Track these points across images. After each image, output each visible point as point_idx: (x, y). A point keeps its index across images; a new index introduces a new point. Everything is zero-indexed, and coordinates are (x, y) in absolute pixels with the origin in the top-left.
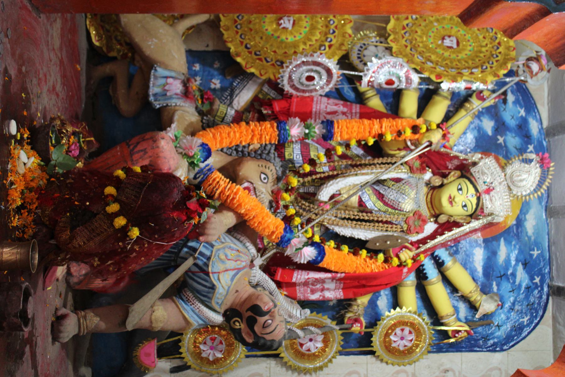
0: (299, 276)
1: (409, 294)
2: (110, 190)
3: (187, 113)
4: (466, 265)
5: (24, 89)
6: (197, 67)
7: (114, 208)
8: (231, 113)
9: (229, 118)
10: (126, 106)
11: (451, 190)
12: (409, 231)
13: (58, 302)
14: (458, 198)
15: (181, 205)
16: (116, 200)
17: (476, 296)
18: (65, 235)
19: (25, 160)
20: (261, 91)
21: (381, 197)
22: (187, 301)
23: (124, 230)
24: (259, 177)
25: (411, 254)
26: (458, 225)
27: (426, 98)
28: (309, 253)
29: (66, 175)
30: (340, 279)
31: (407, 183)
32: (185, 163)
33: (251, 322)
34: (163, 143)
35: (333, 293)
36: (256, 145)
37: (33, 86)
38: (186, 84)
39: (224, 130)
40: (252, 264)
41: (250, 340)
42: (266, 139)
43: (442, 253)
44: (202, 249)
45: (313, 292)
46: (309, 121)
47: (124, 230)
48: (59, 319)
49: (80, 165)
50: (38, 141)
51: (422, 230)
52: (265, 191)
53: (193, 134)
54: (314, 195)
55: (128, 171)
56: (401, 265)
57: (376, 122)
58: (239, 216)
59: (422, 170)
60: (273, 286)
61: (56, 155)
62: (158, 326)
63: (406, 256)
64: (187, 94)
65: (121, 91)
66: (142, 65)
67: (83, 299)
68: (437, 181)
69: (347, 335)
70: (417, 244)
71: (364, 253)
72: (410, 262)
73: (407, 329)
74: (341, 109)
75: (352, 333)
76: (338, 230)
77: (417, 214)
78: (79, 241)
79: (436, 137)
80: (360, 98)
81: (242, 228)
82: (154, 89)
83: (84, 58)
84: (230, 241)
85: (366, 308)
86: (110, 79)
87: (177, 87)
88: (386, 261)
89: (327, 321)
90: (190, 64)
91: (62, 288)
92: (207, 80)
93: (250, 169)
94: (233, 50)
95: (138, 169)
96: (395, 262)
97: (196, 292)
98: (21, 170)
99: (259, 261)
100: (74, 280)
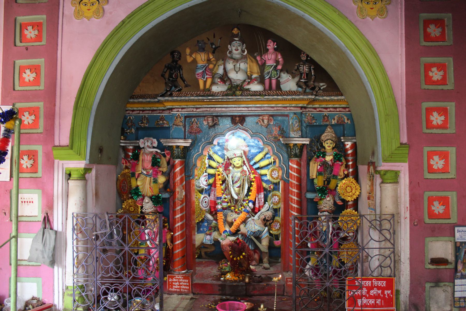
0: (257, 206)
1: (263, 172)
2: (235, 259)
3: (215, 234)
4: (256, 155)
5: (214, 276)
6: (201, 229)
7: (238, 258)
8: (214, 222)
9: (216, 222)
10: (213, 249)
11: (235, 164)
12: (246, 175)
13: (261, 268)
14: (237, 162)
15: (238, 244)
16: (237, 258)
17: (264, 153)
18: (244, 268)
19: (229, 276)
20: (208, 212)
21: (236, 182)
22: (262, 237)
23: (243, 256)
24: (232, 216)
25: (252, 175)
26: (244, 161)
27: (210, 167)
28: (251, 205)
29: (232, 268)
30: (258, 194)
31: (233, 174)
32: (228, 237)
33: (267, 221)
34: (224, 243)
35: (262, 195)
36: (223, 217)
37: (212, 274)
38: (207, 235)
39: (220, 226)
40: (254, 220)
41: (272, 221)
42: (221, 215)
43: (252, 163)
44: (248, 234)
45: (261, 201)
46: (217, 202)
47: (243, 256)
48: (265, 268)
49: (229, 263)
50: (224, 274)
51: (246, 171)
52: (235, 215)
53: (221, 234)
54: (236, 200)
55: (231, 254)
56: (255, 177)
57: (217, 185)
58: (241, 223)
59: (229, 170)
60: (259, 213)
61: (227, 270)
62: (268, 244)
63: (252, 176)
64: (210, 234)
65: (208, 250)
66: (203, 246)
67: (261, 261)
68: (233, 166)
69: (274, 189)
70: (250, 173)
71: (251, 188)
72: (254, 175)
73: (273, 173)
74: (213, 192)
75: (274, 188)
76: (245, 194)
77: (241, 172)
78: (245, 266)
79: (221, 169)
80: (210, 185)
81: (244, 222)
82: (209, 243)
83: (201, 260)
84: (247, 226)
85: (267, 184)
86: (206, 253)
87: (208, 237)
88: (253, 182)
89: (270, 195)
90: (201, 232)
91: (258, 267)
92: (205, 226)
93: (229, 219)
94: (198, 221)
95: (230, 252)
96: (254, 179)
97: (260, 234)
98: (231, 277)
99: (253, 218)
100: (256, 264)
